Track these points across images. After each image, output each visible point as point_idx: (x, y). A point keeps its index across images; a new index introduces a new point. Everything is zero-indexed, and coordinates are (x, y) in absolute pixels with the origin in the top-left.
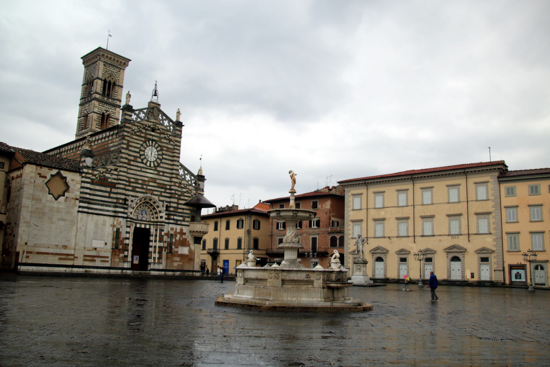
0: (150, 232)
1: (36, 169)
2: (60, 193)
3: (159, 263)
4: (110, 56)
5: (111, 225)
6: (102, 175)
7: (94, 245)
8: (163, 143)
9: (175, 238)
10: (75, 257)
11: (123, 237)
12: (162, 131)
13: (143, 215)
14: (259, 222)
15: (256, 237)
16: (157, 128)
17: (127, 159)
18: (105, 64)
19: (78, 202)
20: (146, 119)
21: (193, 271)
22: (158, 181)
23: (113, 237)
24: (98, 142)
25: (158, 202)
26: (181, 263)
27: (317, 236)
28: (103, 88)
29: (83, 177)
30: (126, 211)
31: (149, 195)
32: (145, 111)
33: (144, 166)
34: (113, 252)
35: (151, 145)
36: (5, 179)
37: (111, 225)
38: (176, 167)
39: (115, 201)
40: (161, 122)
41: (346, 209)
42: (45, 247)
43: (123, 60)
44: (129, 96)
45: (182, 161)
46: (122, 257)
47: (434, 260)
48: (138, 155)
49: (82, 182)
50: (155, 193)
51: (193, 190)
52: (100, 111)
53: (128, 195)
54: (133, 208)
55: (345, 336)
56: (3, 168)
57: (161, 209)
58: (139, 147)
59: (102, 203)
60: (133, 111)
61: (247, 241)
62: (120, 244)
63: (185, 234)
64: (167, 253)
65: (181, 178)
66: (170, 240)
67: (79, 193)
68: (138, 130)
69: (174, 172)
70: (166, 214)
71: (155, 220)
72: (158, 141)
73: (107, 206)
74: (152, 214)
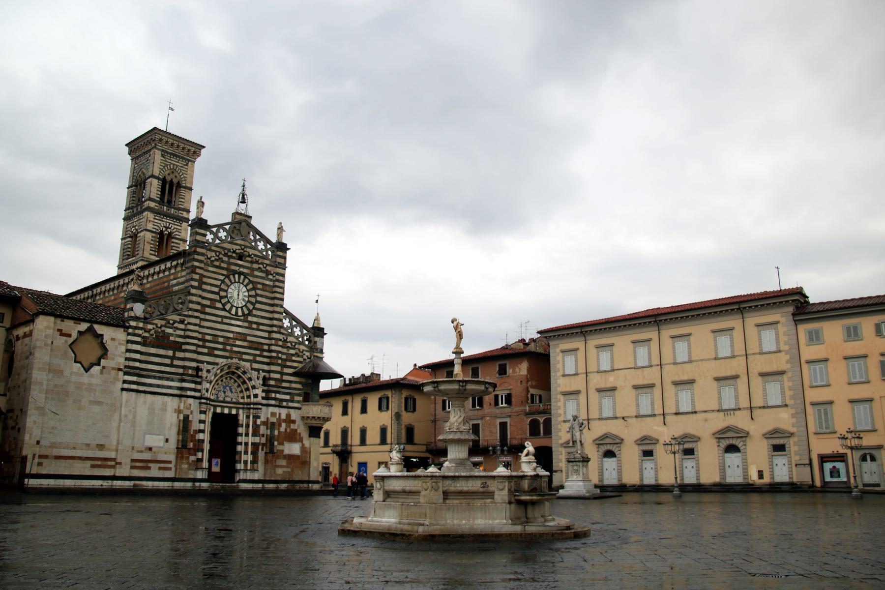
0: (239, 420)
1: (55, 323)
2: (94, 359)
3: (253, 470)
4: (171, 141)
5: (175, 410)
6: (159, 330)
7: (148, 443)
8: (257, 277)
9: (279, 429)
10: (117, 463)
11: (195, 429)
12: (254, 258)
13: (227, 394)
14: (415, 400)
15: (410, 425)
16: (247, 254)
17: (199, 303)
18: (164, 153)
19: (121, 373)
20: (229, 239)
21: (309, 482)
22: (249, 338)
23: (179, 429)
24: (153, 278)
25: (250, 371)
26: (289, 470)
27: (508, 420)
28: (161, 192)
29: (129, 334)
30: (199, 387)
31: (235, 361)
32: (227, 227)
33: (227, 314)
34: (178, 453)
35: (237, 280)
36: (6, 340)
37: (175, 410)
38: (279, 315)
39: (181, 371)
40: (253, 244)
41: (552, 374)
42: (68, 448)
43: (192, 147)
44: (201, 204)
45: (288, 304)
46: (193, 461)
47: (656, 453)
49: (128, 342)
50: (245, 357)
51: (307, 351)
52: (156, 227)
53: (202, 362)
54: (211, 382)
55: (537, 577)
56: (2, 322)
57: (255, 382)
58: (219, 284)
59: (161, 375)
60: (208, 228)
61: (396, 431)
62: (189, 440)
63: (294, 422)
64: (266, 453)
65: (286, 333)
66: (271, 431)
67: (124, 359)
68: (217, 258)
69: (275, 322)
70: (263, 391)
71: (246, 400)
72: (248, 274)
73: (168, 379)
74: (241, 391)
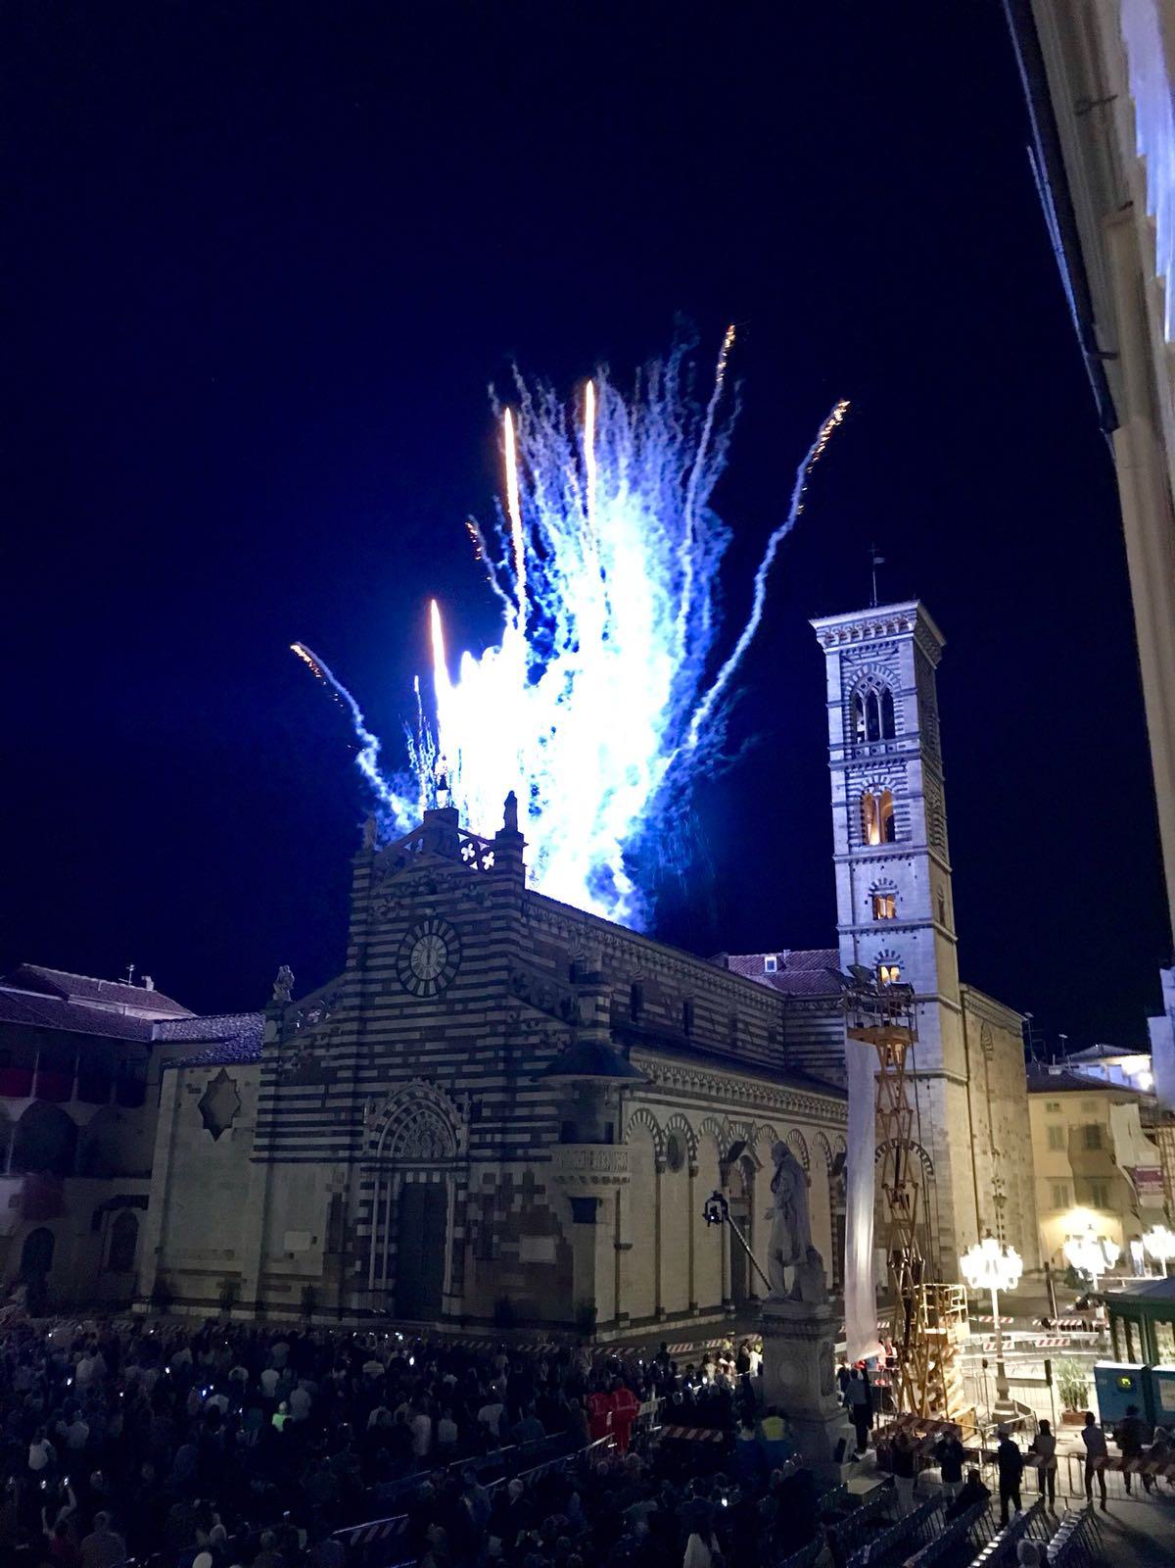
7: (289, 1247)
8: (463, 912)
22: (449, 1033)
35: (427, 932)
38: (498, 973)
48: (392, 974)
50: (441, 1070)
51: (563, 1032)
54: (380, 1129)
63: (541, 1190)
70: (472, 1132)
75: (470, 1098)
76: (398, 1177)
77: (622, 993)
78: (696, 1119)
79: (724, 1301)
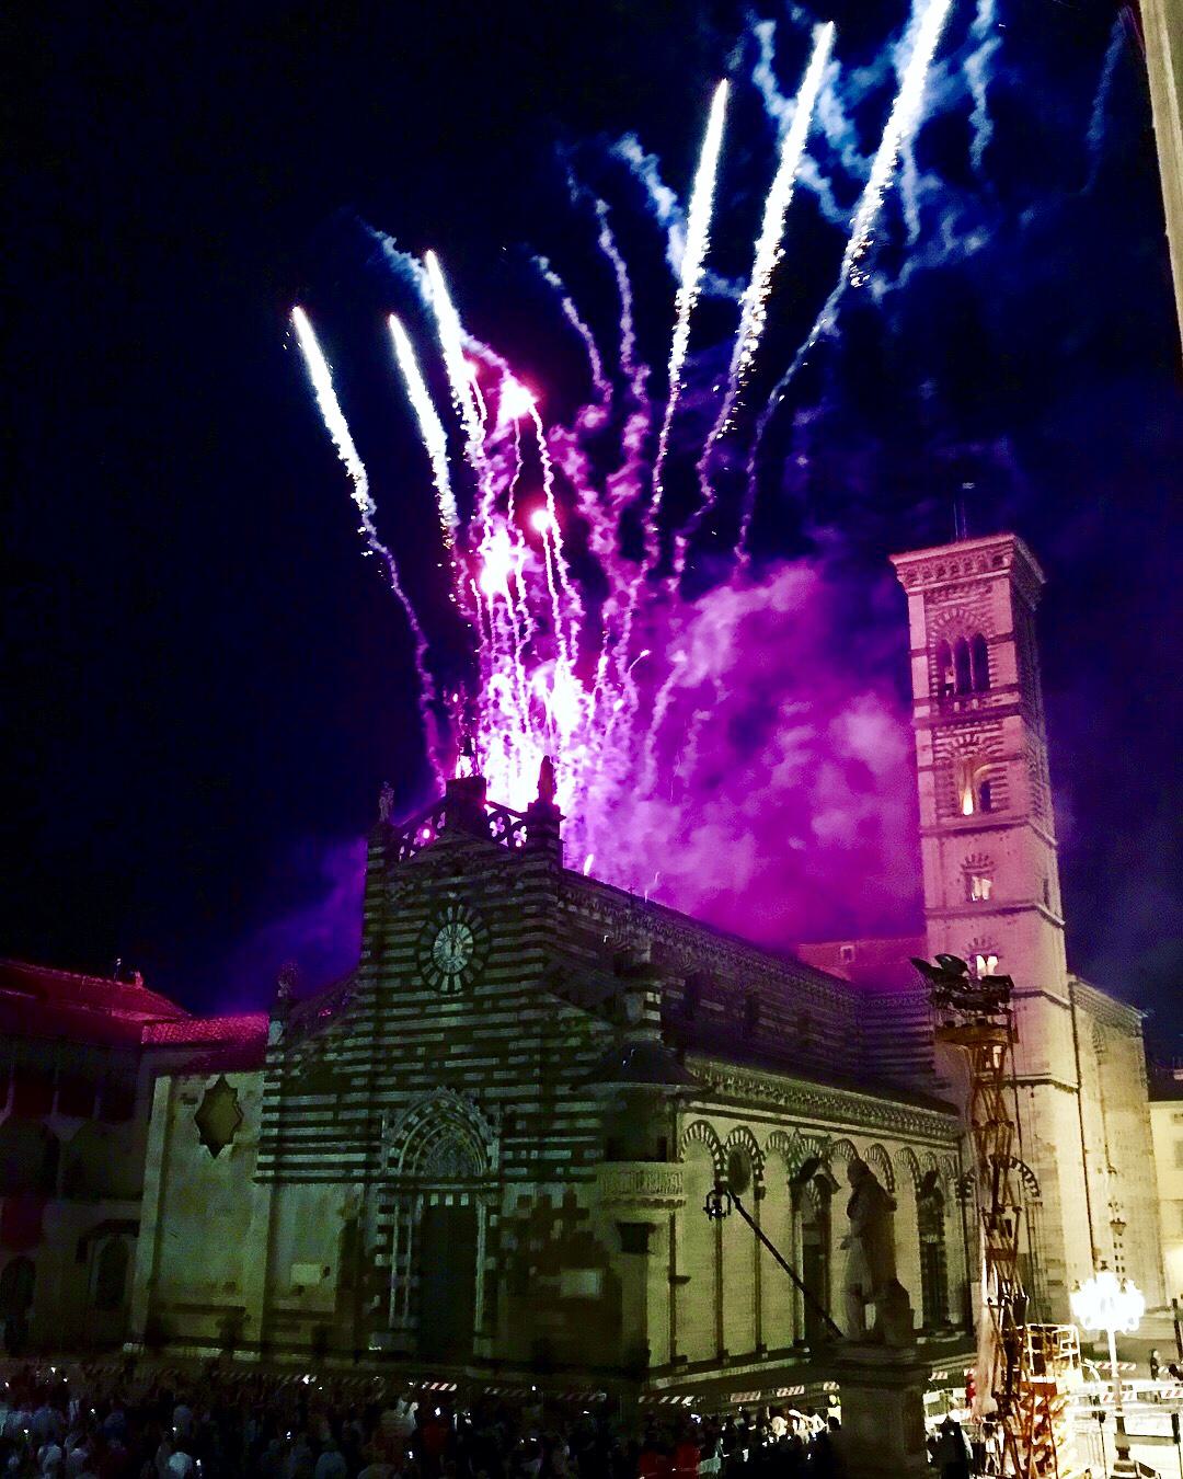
8: (491, 896)
33: (434, 995)
48: (413, 966)
50: (470, 1077)
54: (399, 1144)
63: (584, 1214)
70: (503, 1148)
75: (502, 1109)
76: (420, 1201)
77: (678, 988)
78: (762, 1132)
79: (797, 1342)
